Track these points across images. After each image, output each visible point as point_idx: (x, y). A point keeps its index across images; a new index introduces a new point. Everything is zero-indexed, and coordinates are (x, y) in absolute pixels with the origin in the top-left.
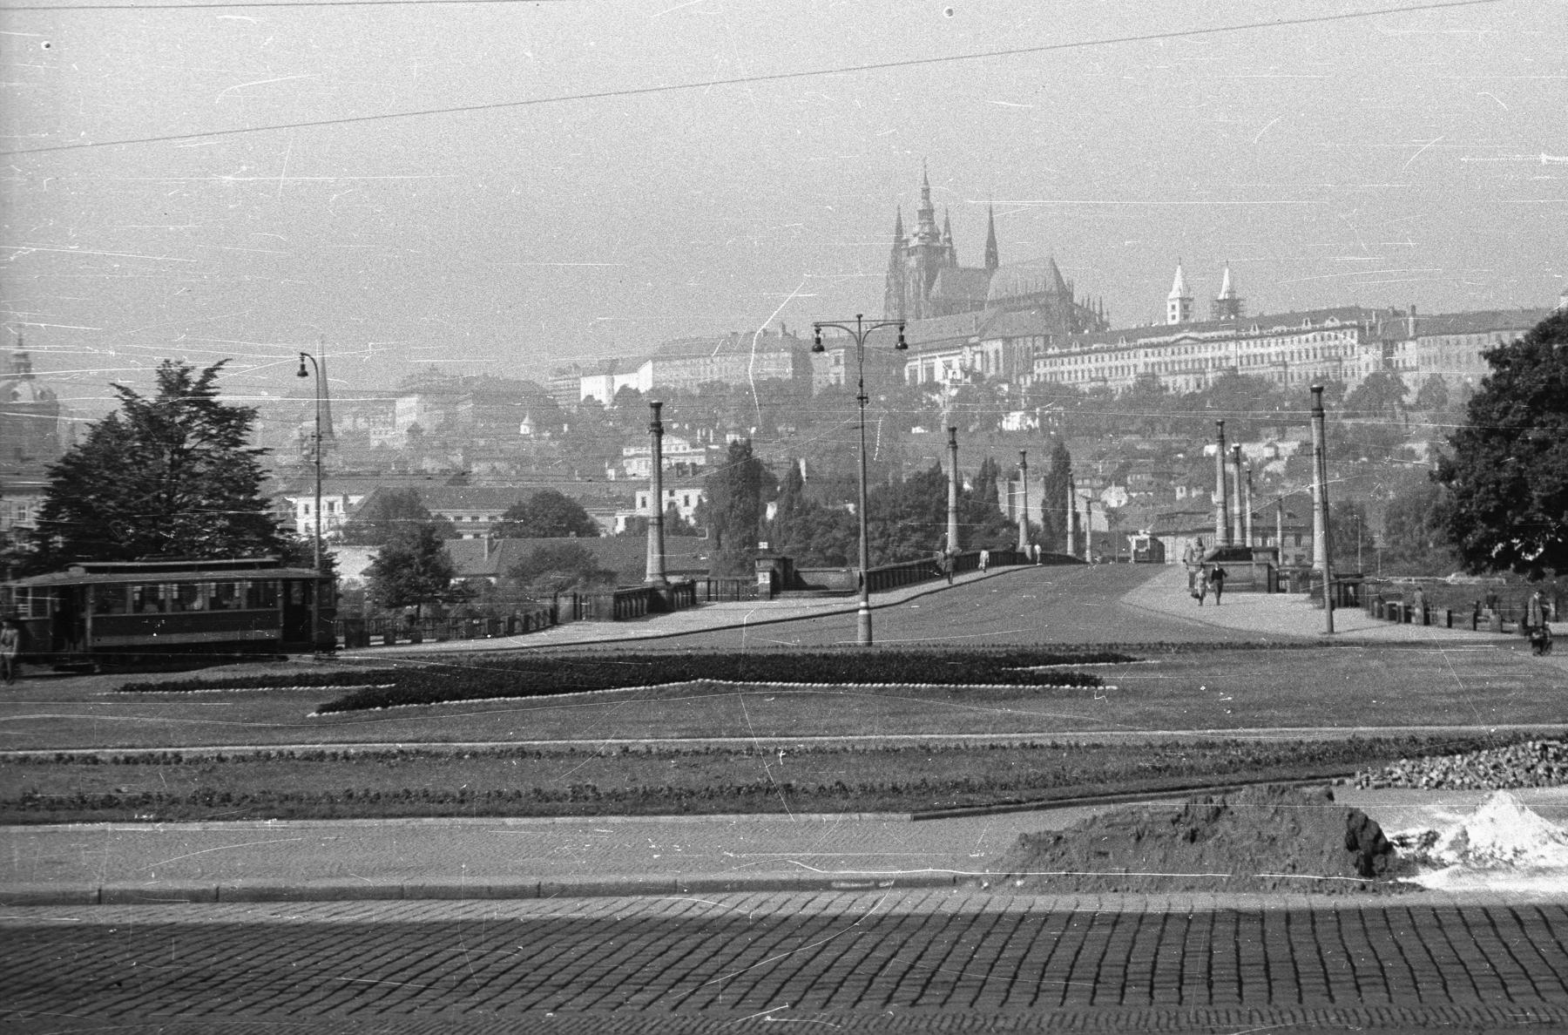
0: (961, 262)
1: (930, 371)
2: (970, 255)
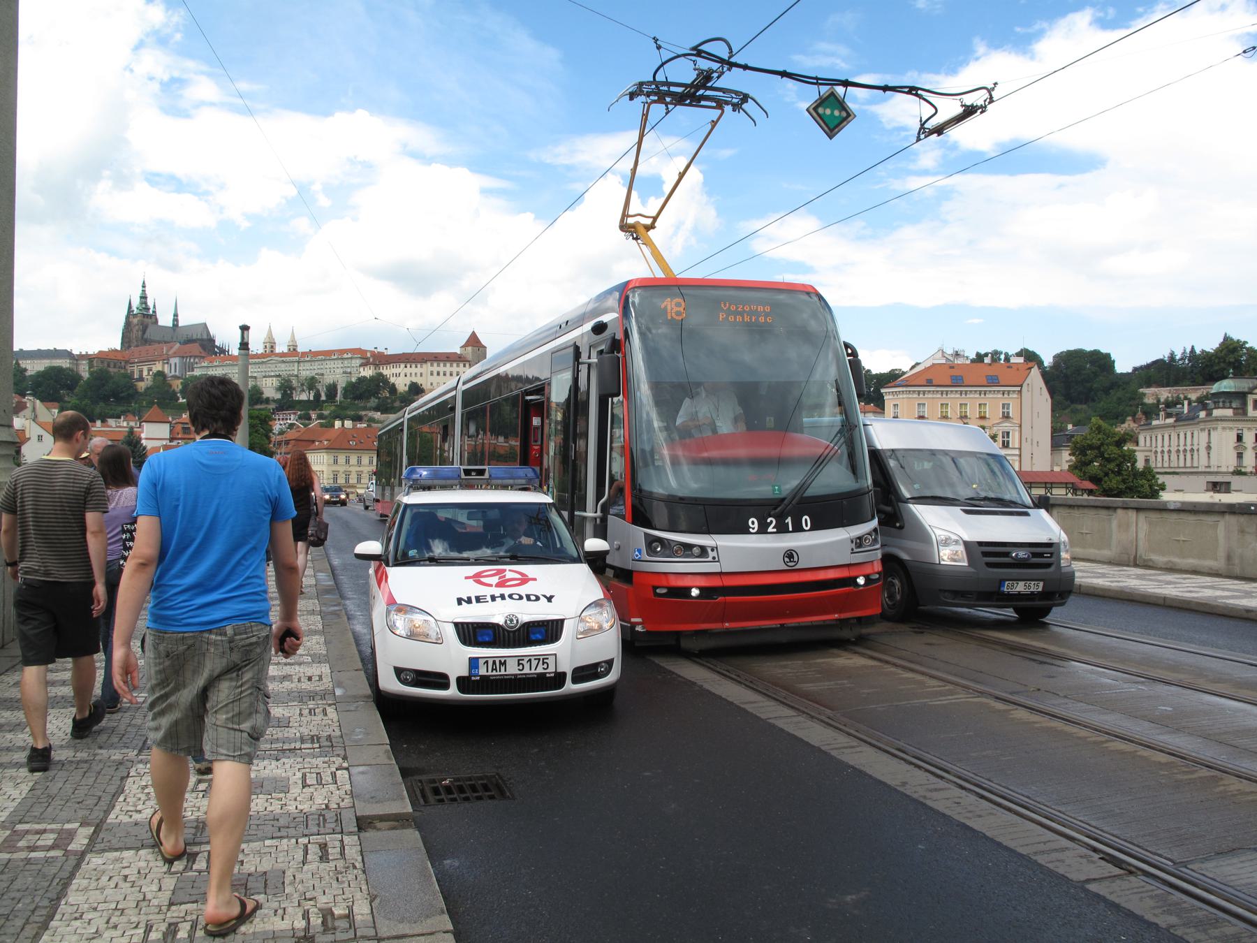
0: (160, 324)
1: (141, 371)
2: (165, 320)
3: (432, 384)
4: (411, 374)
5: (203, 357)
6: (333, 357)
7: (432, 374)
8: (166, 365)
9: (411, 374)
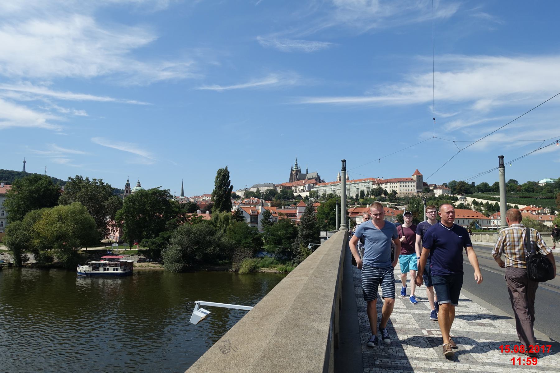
0: (302, 173)
1: (296, 190)
2: (303, 172)
3: (401, 190)
4: (392, 187)
5: (317, 184)
6: (362, 182)
7: (401, 186)
8: (304, 187)
9: (392, 187)
